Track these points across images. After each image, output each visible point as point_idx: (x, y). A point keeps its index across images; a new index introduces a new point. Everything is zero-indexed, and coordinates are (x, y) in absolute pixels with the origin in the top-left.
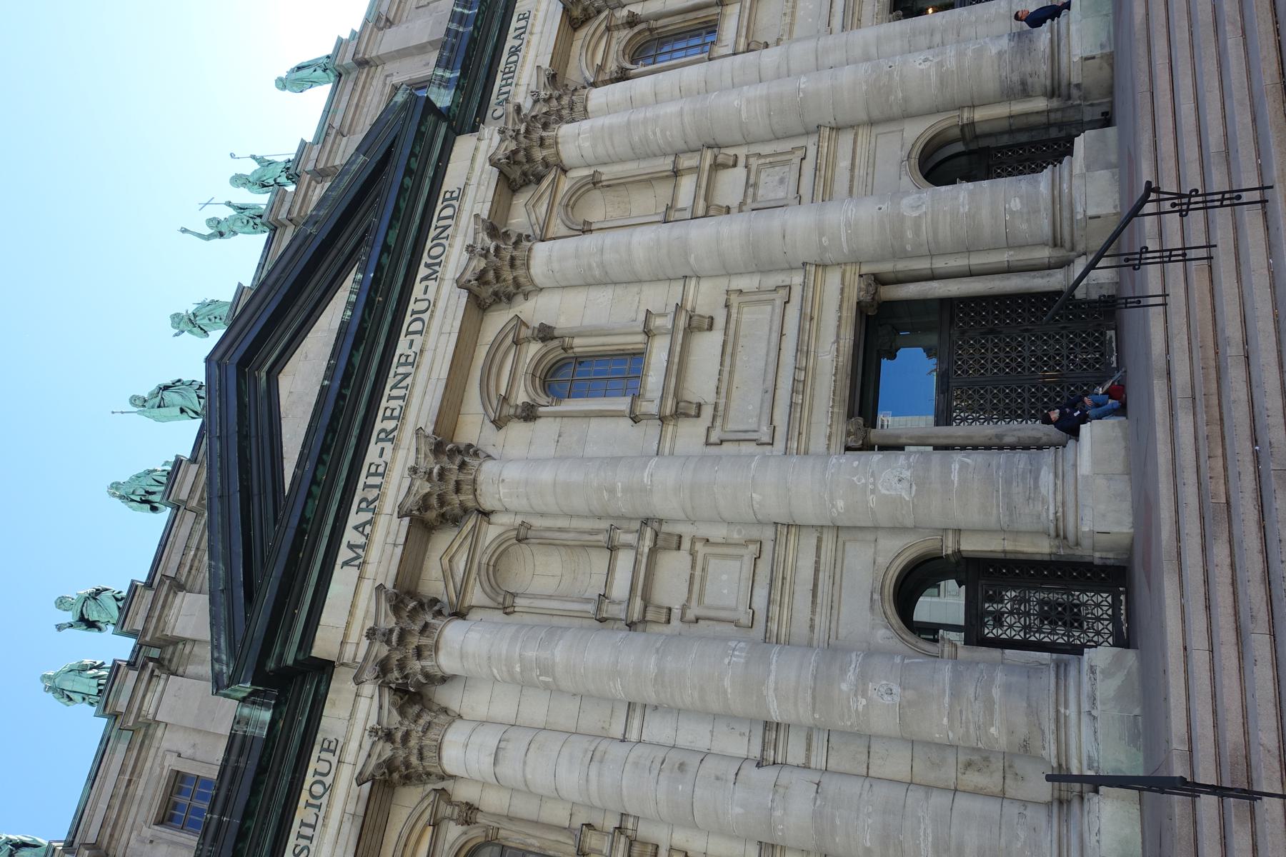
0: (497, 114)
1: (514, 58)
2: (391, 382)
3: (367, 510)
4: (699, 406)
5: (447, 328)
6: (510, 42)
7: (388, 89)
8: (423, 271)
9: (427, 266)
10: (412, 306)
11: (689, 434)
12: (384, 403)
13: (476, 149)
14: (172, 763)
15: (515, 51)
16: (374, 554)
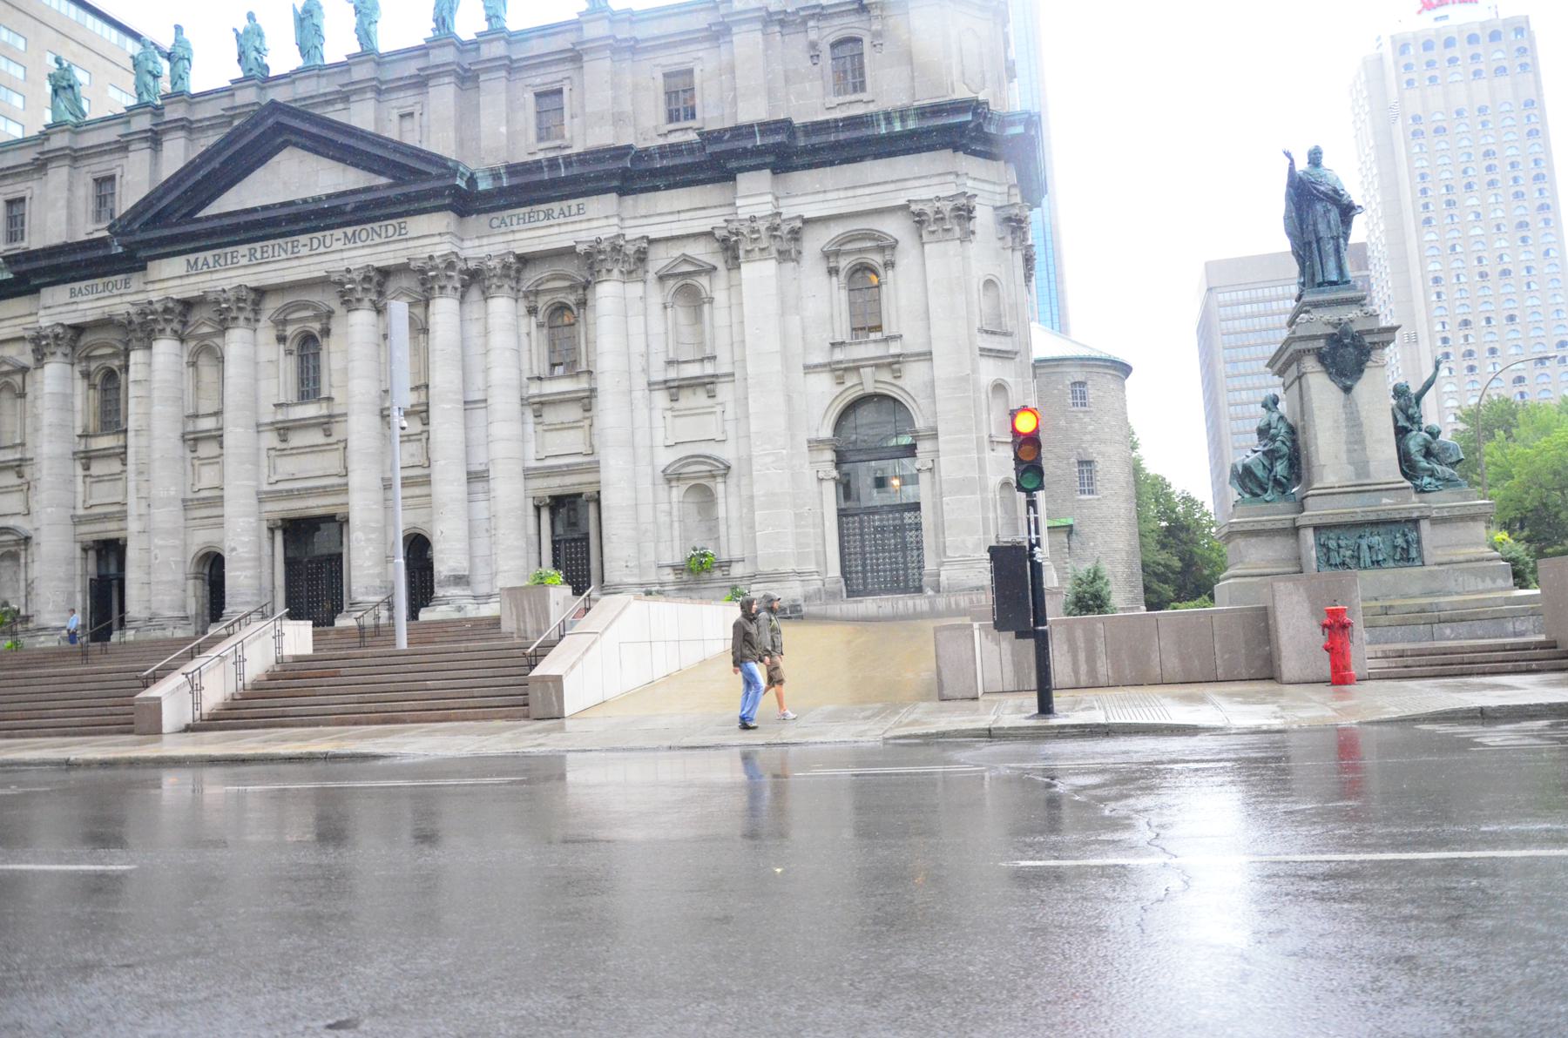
0: (495, 223)
1: (542, 216)
2: (280, 241)
3: (215, 261)
4: (284, 441)
5: (312, 268)
6: (556, 206)
7: (557, 86)
8: (349, 230)
9: (354, 234)
10: (327, 233)
11: (270, 439)
12: (272, 242)
13: (433, 235)
14: (118, 172)
15: (548, 216)
16: (193, 280)
